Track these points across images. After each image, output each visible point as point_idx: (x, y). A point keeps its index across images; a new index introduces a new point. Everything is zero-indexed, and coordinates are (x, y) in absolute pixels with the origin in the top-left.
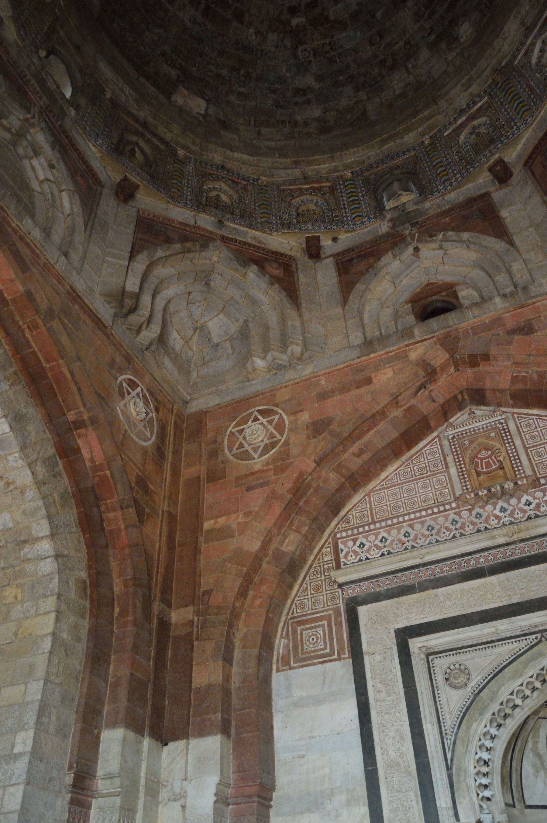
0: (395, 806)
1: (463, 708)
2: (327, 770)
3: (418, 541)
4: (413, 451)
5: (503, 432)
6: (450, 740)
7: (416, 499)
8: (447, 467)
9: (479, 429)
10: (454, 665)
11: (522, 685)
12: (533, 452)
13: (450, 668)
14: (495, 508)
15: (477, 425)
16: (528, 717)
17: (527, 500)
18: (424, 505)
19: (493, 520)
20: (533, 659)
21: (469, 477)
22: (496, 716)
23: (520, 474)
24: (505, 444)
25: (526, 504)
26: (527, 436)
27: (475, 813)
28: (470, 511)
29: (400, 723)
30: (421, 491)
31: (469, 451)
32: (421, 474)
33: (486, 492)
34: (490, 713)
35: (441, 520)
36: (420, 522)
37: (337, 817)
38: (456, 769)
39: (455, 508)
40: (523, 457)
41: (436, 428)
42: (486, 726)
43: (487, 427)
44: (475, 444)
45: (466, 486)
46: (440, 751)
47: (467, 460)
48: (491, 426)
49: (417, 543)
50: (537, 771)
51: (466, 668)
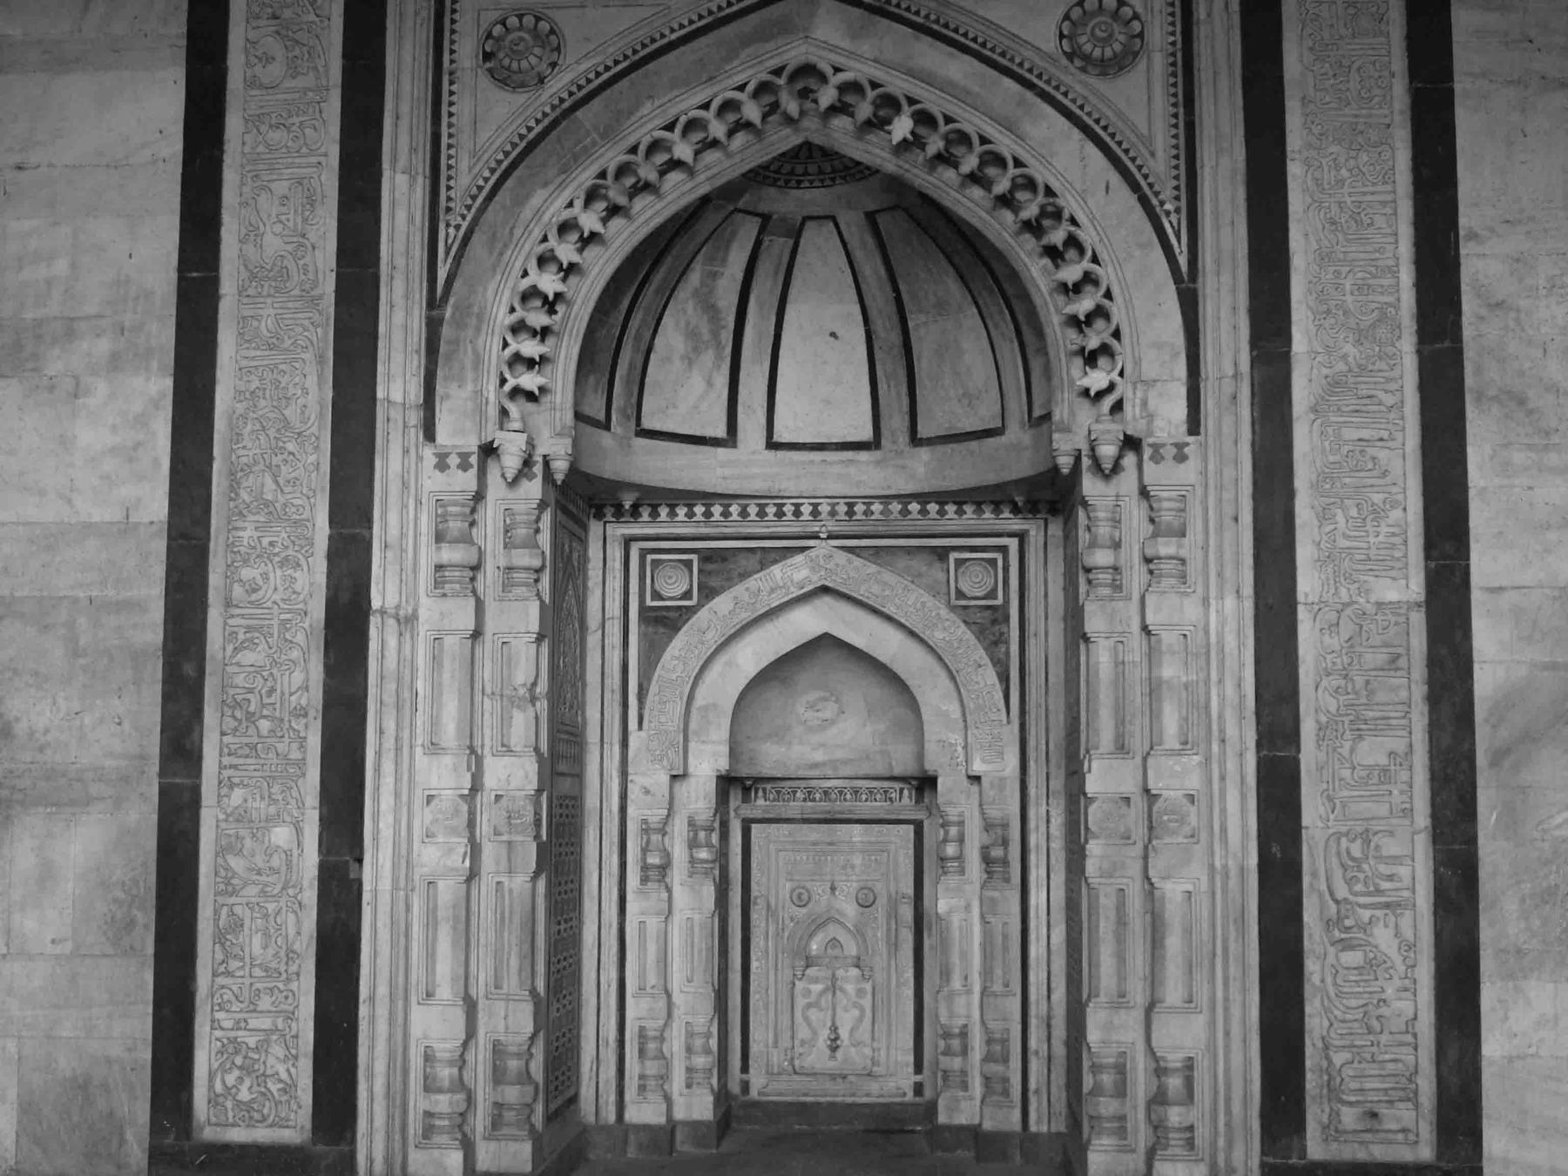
0: (253, 386)
1: (514, 145)
2: (61, 266)
6: (458, 227)
10: (520, 17)
16: (705, 200)
20: (762, 35)
22: (610, 180)
27: (481, 427)
29: (313, 160)
34: (594, 169)
37: (76, 396)
38: (456, 308)
42: (570, 205)
46: (419, 253)
50: (696, 349)
51: (552, 32)
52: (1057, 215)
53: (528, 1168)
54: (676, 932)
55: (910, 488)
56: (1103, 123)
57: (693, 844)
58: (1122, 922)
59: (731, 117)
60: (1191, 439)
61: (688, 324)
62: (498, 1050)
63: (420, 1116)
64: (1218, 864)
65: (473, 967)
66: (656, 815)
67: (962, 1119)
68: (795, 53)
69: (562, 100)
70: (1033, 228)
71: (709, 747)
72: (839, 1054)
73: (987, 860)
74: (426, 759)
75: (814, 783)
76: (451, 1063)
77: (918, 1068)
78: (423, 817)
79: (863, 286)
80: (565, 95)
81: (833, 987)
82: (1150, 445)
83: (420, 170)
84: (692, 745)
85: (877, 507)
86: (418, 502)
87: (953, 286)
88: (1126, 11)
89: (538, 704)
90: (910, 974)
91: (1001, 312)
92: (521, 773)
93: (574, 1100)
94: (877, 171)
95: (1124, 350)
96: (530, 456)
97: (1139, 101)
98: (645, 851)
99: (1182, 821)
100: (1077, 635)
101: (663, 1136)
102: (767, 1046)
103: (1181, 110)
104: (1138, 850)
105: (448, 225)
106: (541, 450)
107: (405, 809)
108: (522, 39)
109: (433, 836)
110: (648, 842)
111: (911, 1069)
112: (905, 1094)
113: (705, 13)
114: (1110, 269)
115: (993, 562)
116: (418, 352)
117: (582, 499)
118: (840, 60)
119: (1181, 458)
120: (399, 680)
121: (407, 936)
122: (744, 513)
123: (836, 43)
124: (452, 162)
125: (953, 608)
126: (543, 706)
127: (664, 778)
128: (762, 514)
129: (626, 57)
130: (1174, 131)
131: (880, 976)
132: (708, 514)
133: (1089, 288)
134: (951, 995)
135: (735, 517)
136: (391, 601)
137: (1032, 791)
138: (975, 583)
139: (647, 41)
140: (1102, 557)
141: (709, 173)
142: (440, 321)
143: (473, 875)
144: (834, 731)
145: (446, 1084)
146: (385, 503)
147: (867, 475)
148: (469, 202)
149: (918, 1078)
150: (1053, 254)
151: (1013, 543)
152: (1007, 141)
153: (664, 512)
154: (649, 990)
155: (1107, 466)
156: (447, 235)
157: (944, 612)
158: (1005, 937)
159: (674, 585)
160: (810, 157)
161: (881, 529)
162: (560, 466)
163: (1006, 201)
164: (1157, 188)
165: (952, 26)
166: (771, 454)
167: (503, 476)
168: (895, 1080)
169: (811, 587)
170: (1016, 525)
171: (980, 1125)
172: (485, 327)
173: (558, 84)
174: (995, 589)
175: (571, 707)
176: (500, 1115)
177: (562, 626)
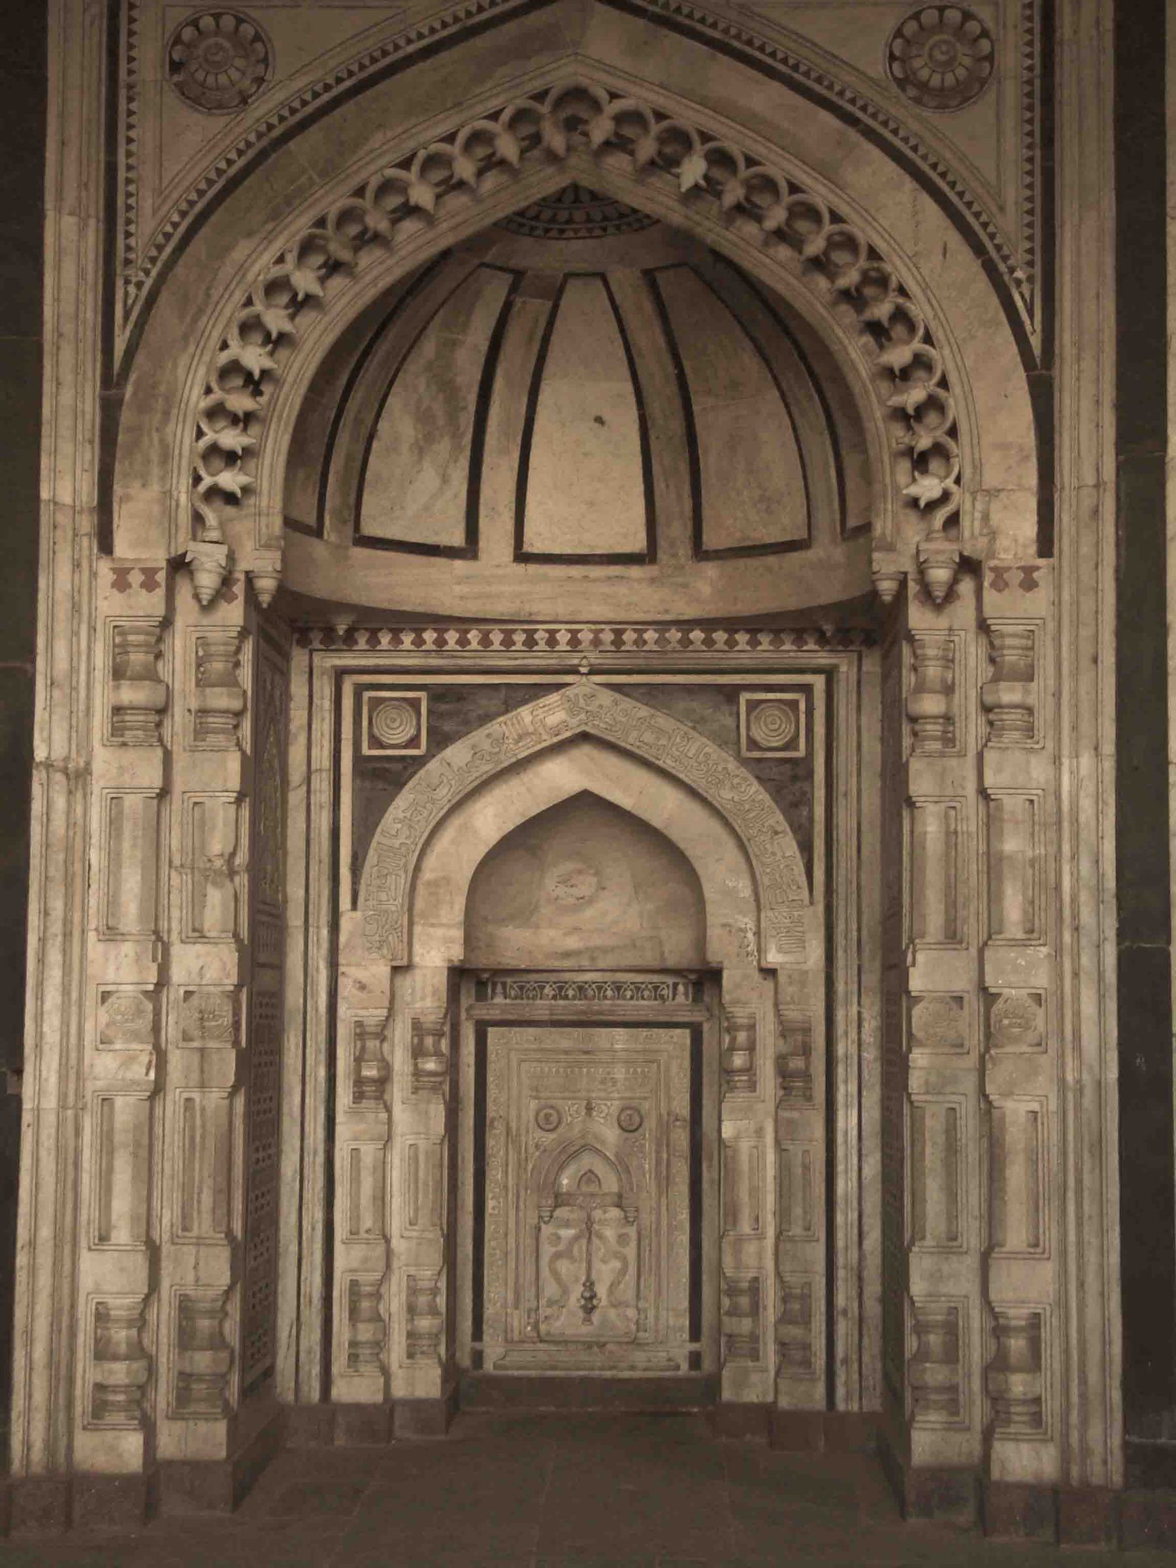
1: (210, 183)
6: (139, 285)
10: (217, 17)
11: (450, 138)
13: (195, 23)
16: (446, 254)
22: (330, 230)
42: (281, 260)
46: (91, 315)
51: (257, 38)
52: (883, 281)
53: (223, 1454)
54: (396, 1162)
55: (690, 613)
56: (941, 168)
57: (418, 1052)
58: (952, 1148)
59: (481, 152)
60: (1041, 562)
61: (419, 401)
62: (186, 1308)
63: (89, 1388)
64: (1070, 1078)
65: (156, 1203)
66: (374, 1015)
67: (752, 1396)
68: (562, 73)
69: (270, 127)
70: (853, 298)
71: (440, 932)
72: (596, 1317)
73: (784, 1073)
74: (101, 947)
75: (567, 976)
76: (130, 1323)
77: (695, 1334)
78: (96, 1019)
79: (637, 360)
80: (274, 120)
81: (589, 1230)
82: (992, 569)
83: (92, 211)
84: (417, 929)
85: (650, 635)
86: (92, 629)
87: (750, 362)
88: (973, 27)
89: (237, 879)
90: (684, 1216)
91: (811, 398)
92: (216, 964)
93: (269, 1372)
94: (658, 221)
95: (961, 451)
96: (230, 572)
97: (986, 143)
98: (359, 1060)
99: (1026, 1027)
100: (897, 798)
101: (377, 1420)
102: (505, 1306)
103: (1038, 153)
104: (971, 1061)
105: (127, 282)
106: (243, 565)
107: (74, 1009)
108: (220, 47)
109: (110, 1042)
110: (363, 1048)
111: (686, 1336)
112: (678, 1368)
113: (449, 20)
114: (947, 351)
115: (794, 704)
116: (91, 442)
117: (290, 622)
118: (619, 85)
119: (1029, 585)
120: (69, 849)
121: (77, 1165)
122: (485, 641)
123: (609, 56)
124: (132, 201)
125: (744, 762)
126: (242, 880)
127: (384, 970)
128: (508, 642)
129: (351, 74)
130: (1028, 180)
131: (647, 1219)
132: (441, 642)
133: (921, 374)
134: (739, 1241)
135: (474, 645)
136: (59, 752)
137: (840, 988)
138: (770, 731)
139: (377, 54)
140: (931, 705)
141: (453, 222)
142: (119, 402)
143: (158, 1089)
144: (589, 913)
145: (123, 1349)
146: (50, 631)
147: (638, 596)
148: (154, 253)
149: (695, 1346)
150: (877, 330)
151: (819, 682)
152: (822, 190)
153: (385, 639)
154: (364, 1235)
155: (939, 593)
156: (126, 294)
157: (732, 765)
158: (806, 1168)
159: (398, 731)
160: (577, 200)
161: (656, 663)
162: (267, 585)
163: (819, 264)
164: (1006, 251)
165: (757, 43)
166: (520, 568)
167: (197, 597)
168: (668, 1350)
169: (568, 734)
170: (824, 659)
171: (775, 1403)
172: (175, 411)
173: (264, 107)
174: (797, 736)
175: (272, 881)
176: (187, 1389)
177: (263, 785)
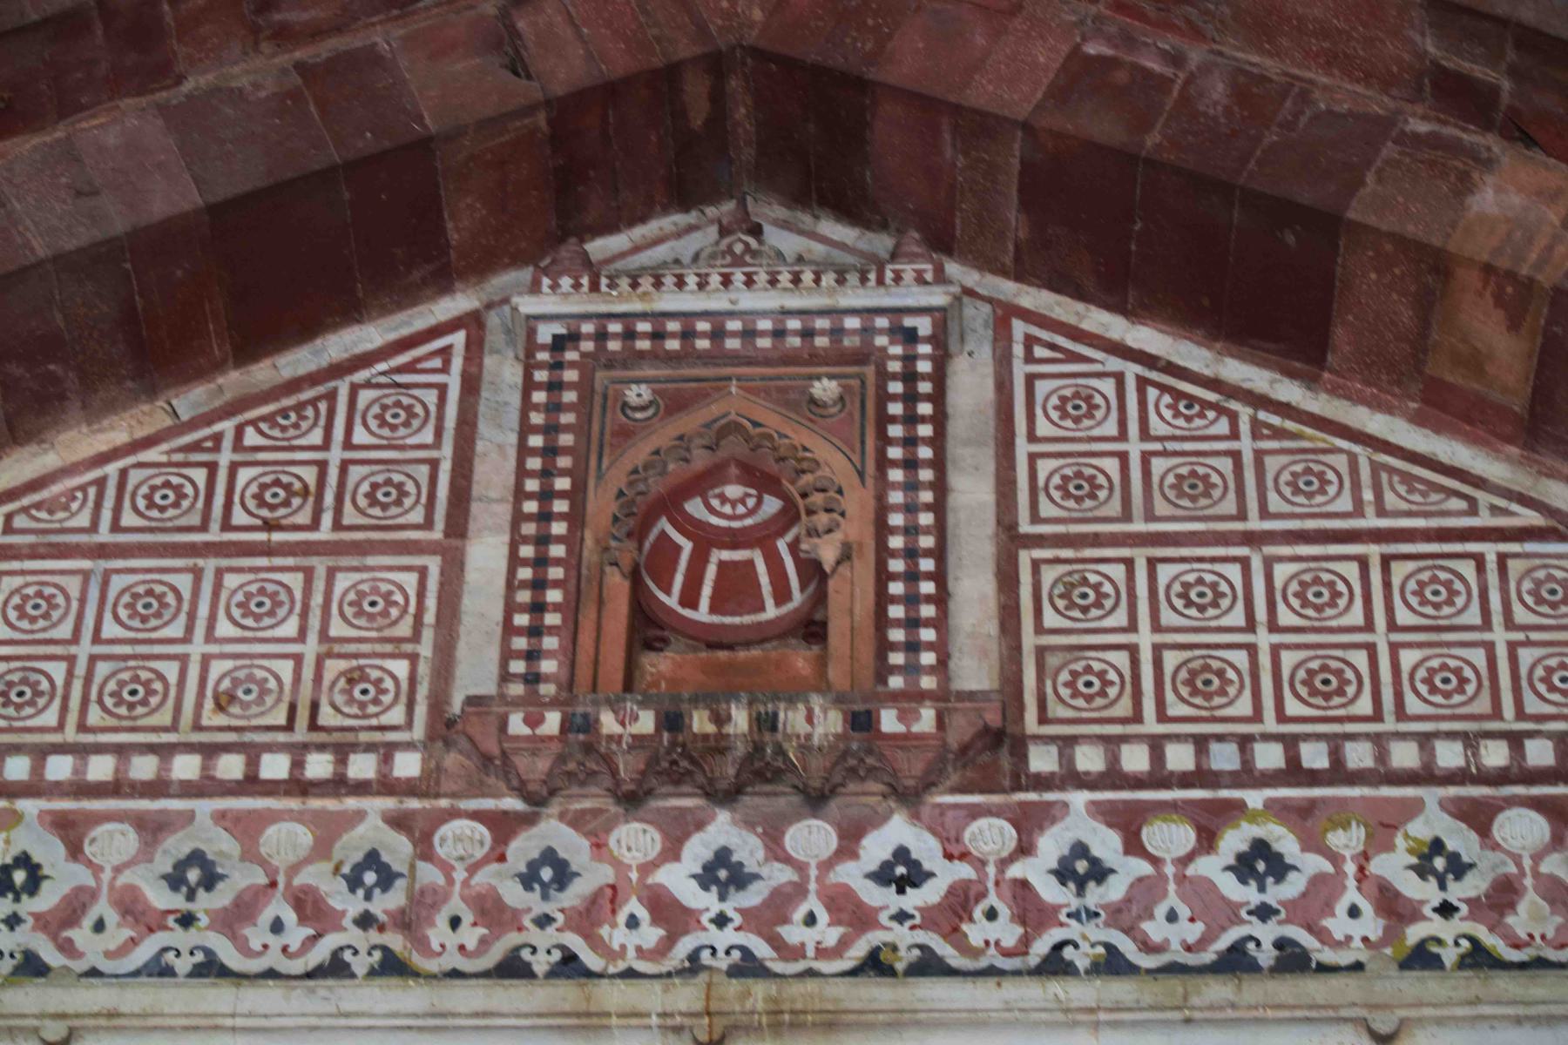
3: (81, 935)
4: (263, 373)
5: (896, 387)
7: (171, 670)
8: (458, 526)
9: (749, 334)
12: (1049, 575)
14: (672, 852)
15: (748, 301)
17: (902, 854)
18: (210, 717)
19: (633, 922)
21: (572, 609)
23: (912, 669)
24: (883, 463)
25: (882, 876)
26: (1044, 467)
28: (503, 827)
30: (224, 628)
31: (639, 453)
32: (269, 526)
33: (646, 723)
35: (287, 838)
36: (141, 823)
39: (409, 788)
40: (974, 589)
41: (480, 265)
43: (807, 334)
44: (689, 422)
45: (532, 656)
47: (601, 504)
48: (837, 332)
49: (68, 948)
